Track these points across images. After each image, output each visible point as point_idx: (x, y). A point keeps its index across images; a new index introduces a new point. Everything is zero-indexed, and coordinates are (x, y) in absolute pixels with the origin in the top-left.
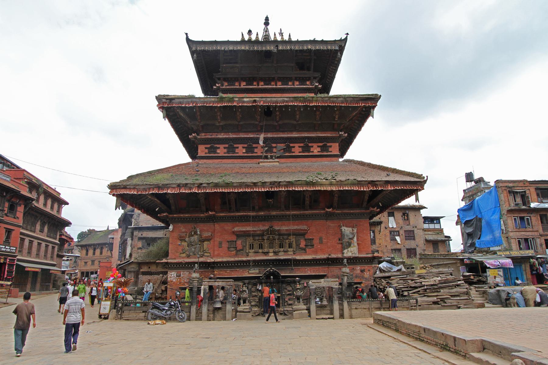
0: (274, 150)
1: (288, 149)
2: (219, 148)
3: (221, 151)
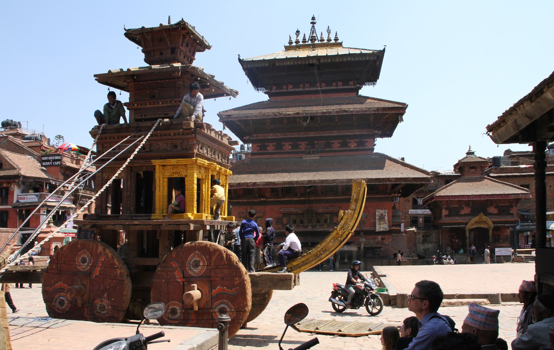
0: (316, 146)
1: (329, 145)
2: (269, 146)
3: (271, 148)
